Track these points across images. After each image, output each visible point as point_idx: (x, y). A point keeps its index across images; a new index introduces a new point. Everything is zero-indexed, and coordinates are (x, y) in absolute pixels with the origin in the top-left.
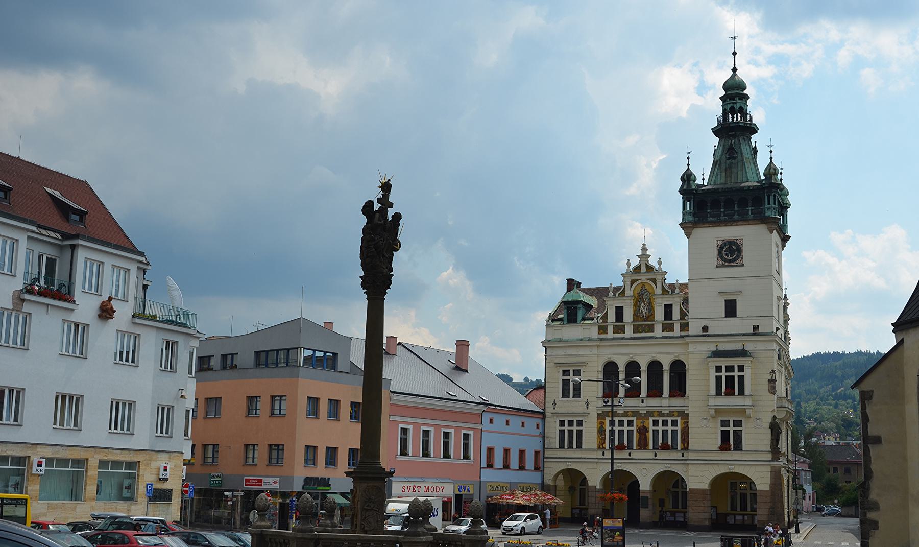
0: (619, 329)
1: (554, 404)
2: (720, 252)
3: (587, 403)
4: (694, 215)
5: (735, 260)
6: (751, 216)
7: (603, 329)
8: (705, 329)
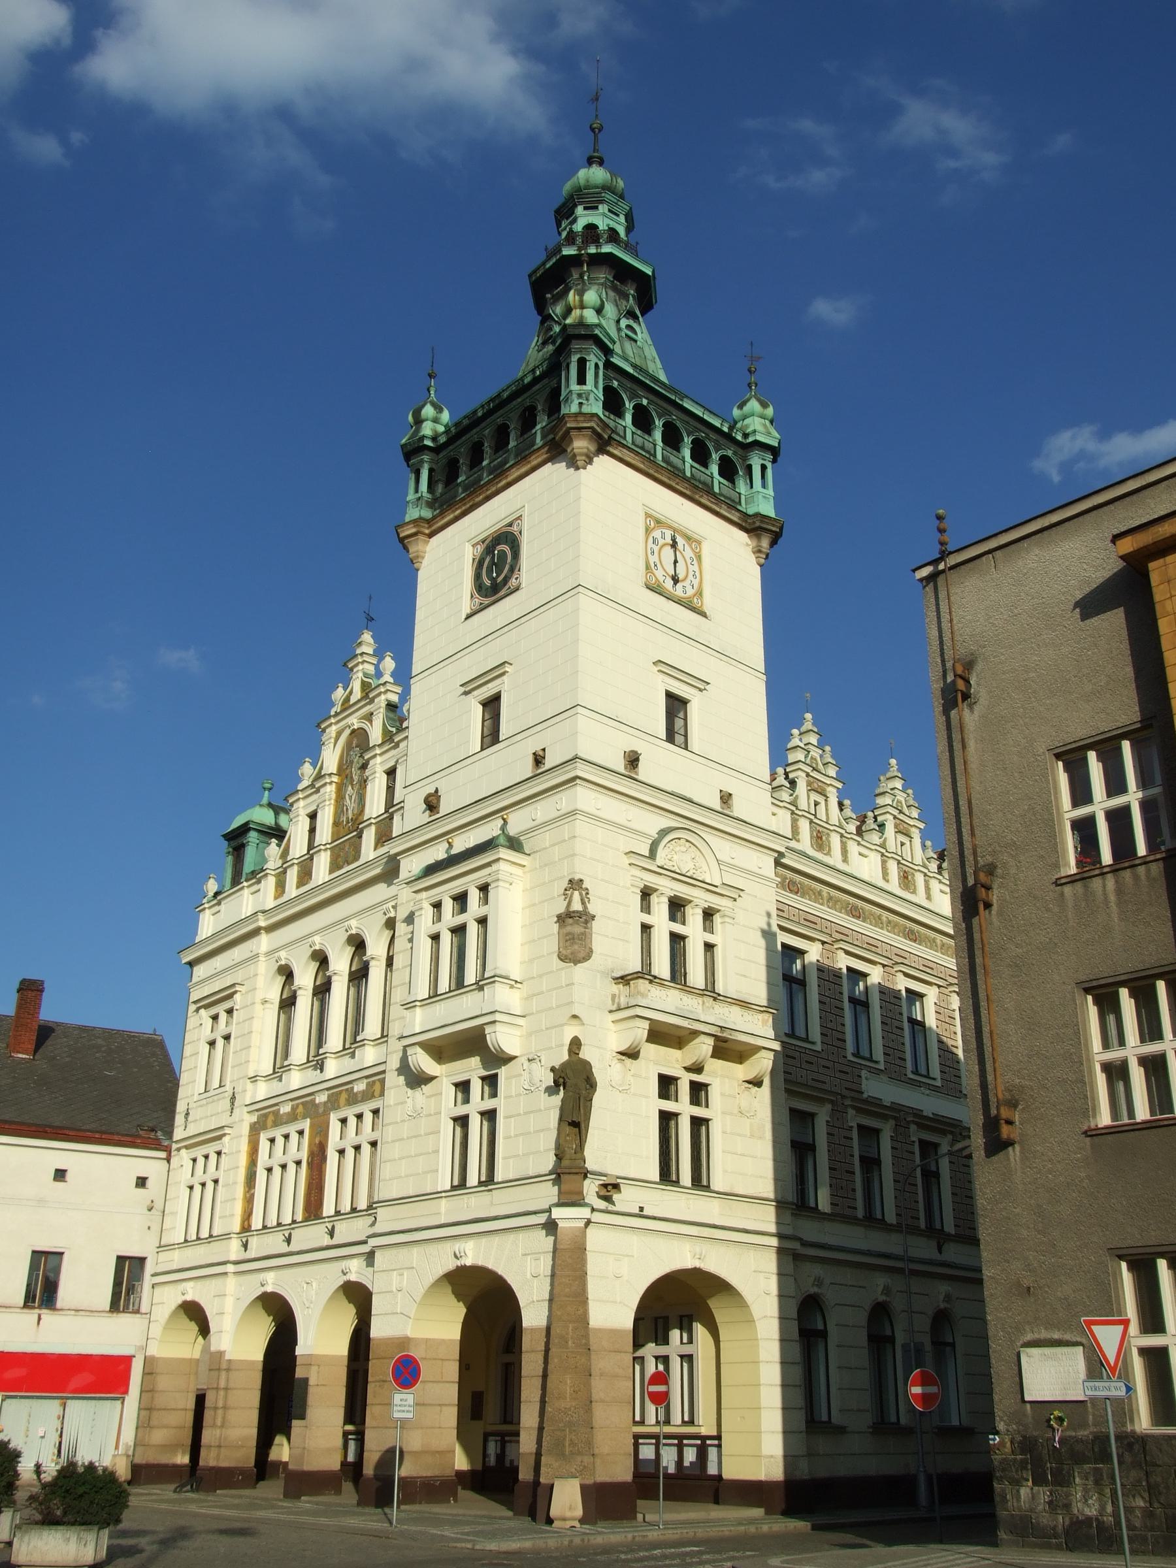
0: (306, 874)
1: (187, 1114)
2: (477, 576)
3: (233, 1098)
4: (431, 505)
5: (506, 580)
6: (539, 441)
7: (281, 886)
8: (432, 804)
